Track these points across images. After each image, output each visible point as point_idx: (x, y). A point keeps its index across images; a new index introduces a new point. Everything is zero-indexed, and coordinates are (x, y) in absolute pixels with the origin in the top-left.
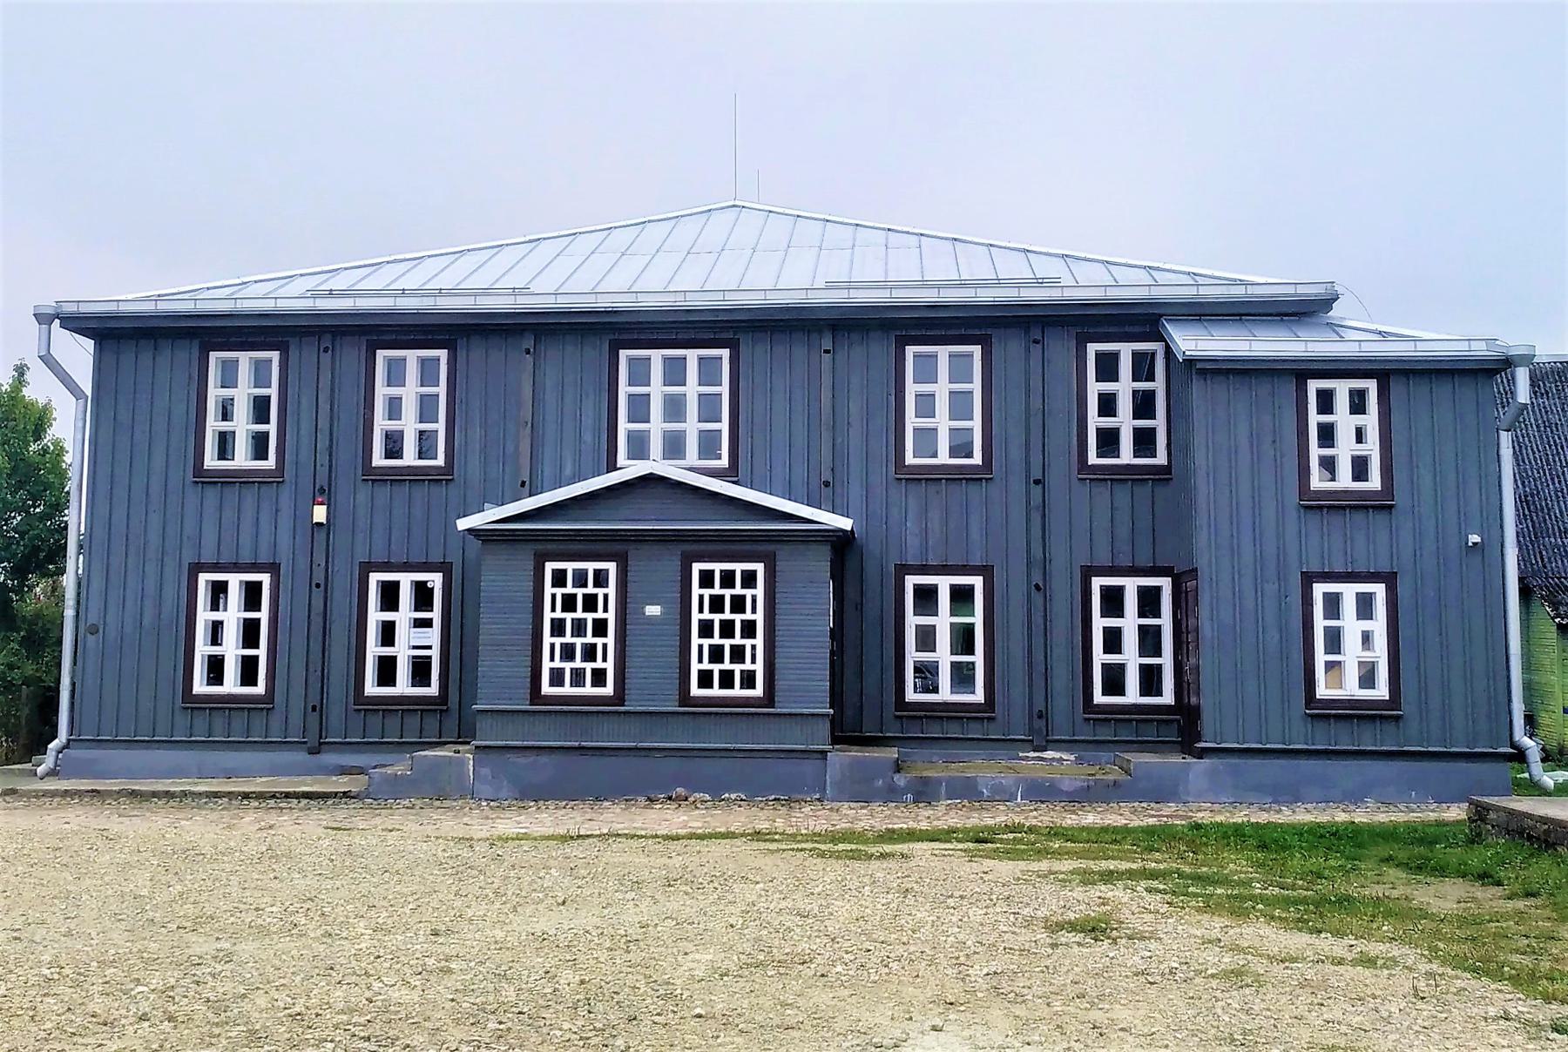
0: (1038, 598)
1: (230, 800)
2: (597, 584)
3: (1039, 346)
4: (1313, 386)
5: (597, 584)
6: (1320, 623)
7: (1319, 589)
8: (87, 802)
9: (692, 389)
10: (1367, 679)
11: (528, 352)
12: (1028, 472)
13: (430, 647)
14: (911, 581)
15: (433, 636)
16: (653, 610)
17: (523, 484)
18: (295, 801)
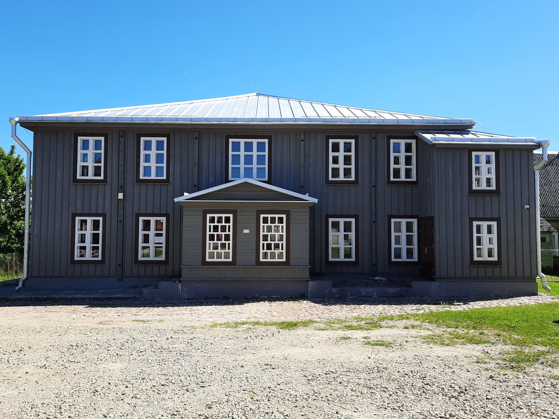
0: (374, 225)
1: (90, 300)
2: (218, 222)
3: (375, 140)
4: (474, 154)
5: (218, 222)
6: (475, 235)
7: (475, 224)
8: (34, 302)
9: (255, 153)
10: (490, 254)
11: (196, 138)
12: (371, 181)
13: (162, 243)
14: (331, 220)
15: (163, 239)
16: (246, 231)
17: (195, 186)
18: (115, 301)
